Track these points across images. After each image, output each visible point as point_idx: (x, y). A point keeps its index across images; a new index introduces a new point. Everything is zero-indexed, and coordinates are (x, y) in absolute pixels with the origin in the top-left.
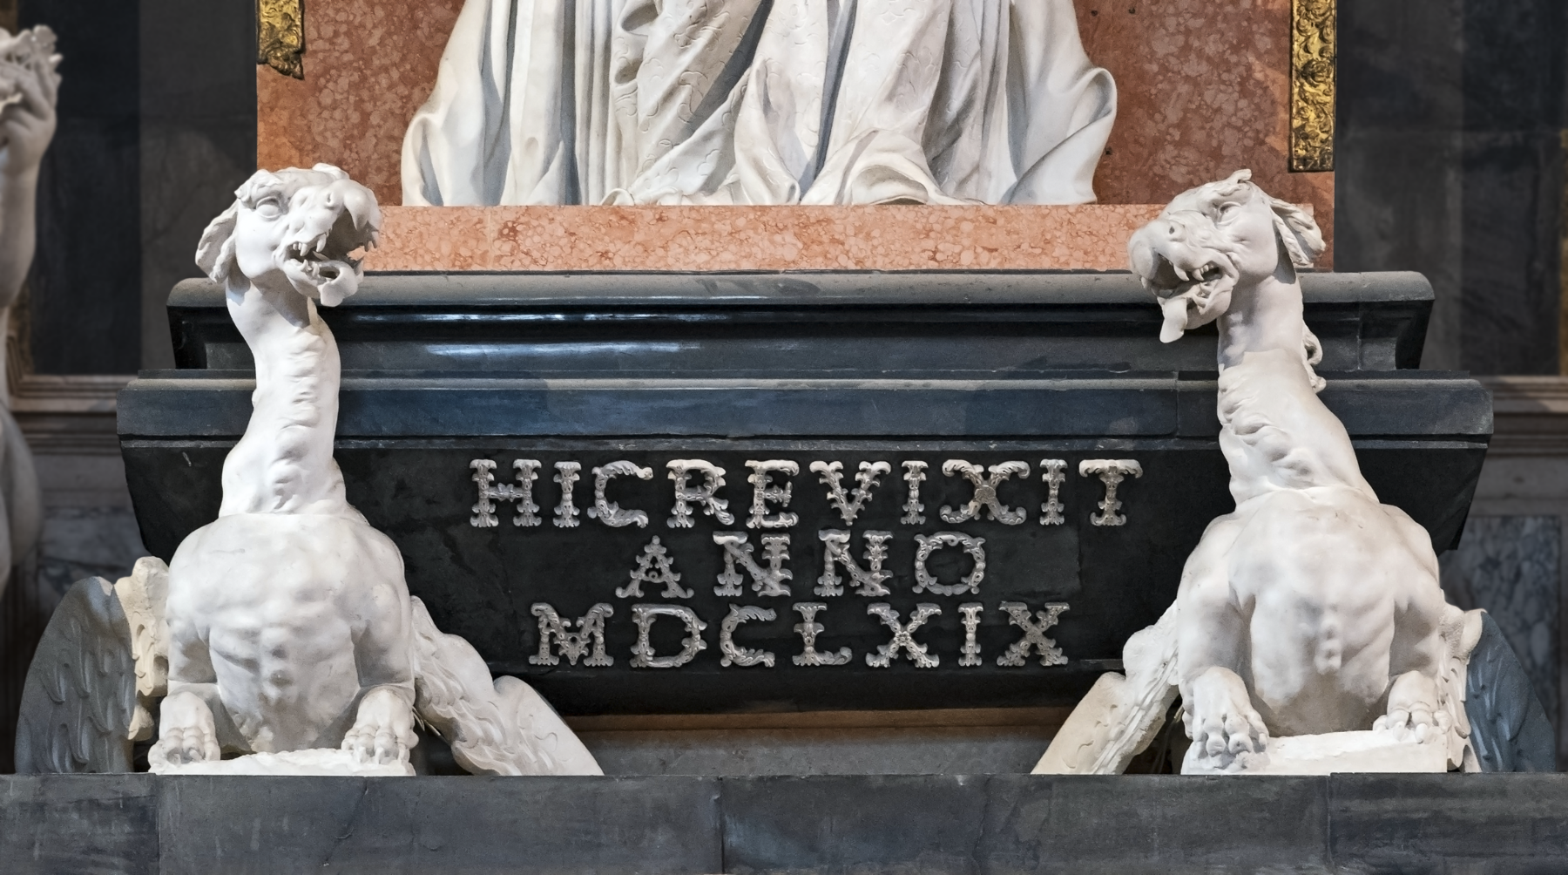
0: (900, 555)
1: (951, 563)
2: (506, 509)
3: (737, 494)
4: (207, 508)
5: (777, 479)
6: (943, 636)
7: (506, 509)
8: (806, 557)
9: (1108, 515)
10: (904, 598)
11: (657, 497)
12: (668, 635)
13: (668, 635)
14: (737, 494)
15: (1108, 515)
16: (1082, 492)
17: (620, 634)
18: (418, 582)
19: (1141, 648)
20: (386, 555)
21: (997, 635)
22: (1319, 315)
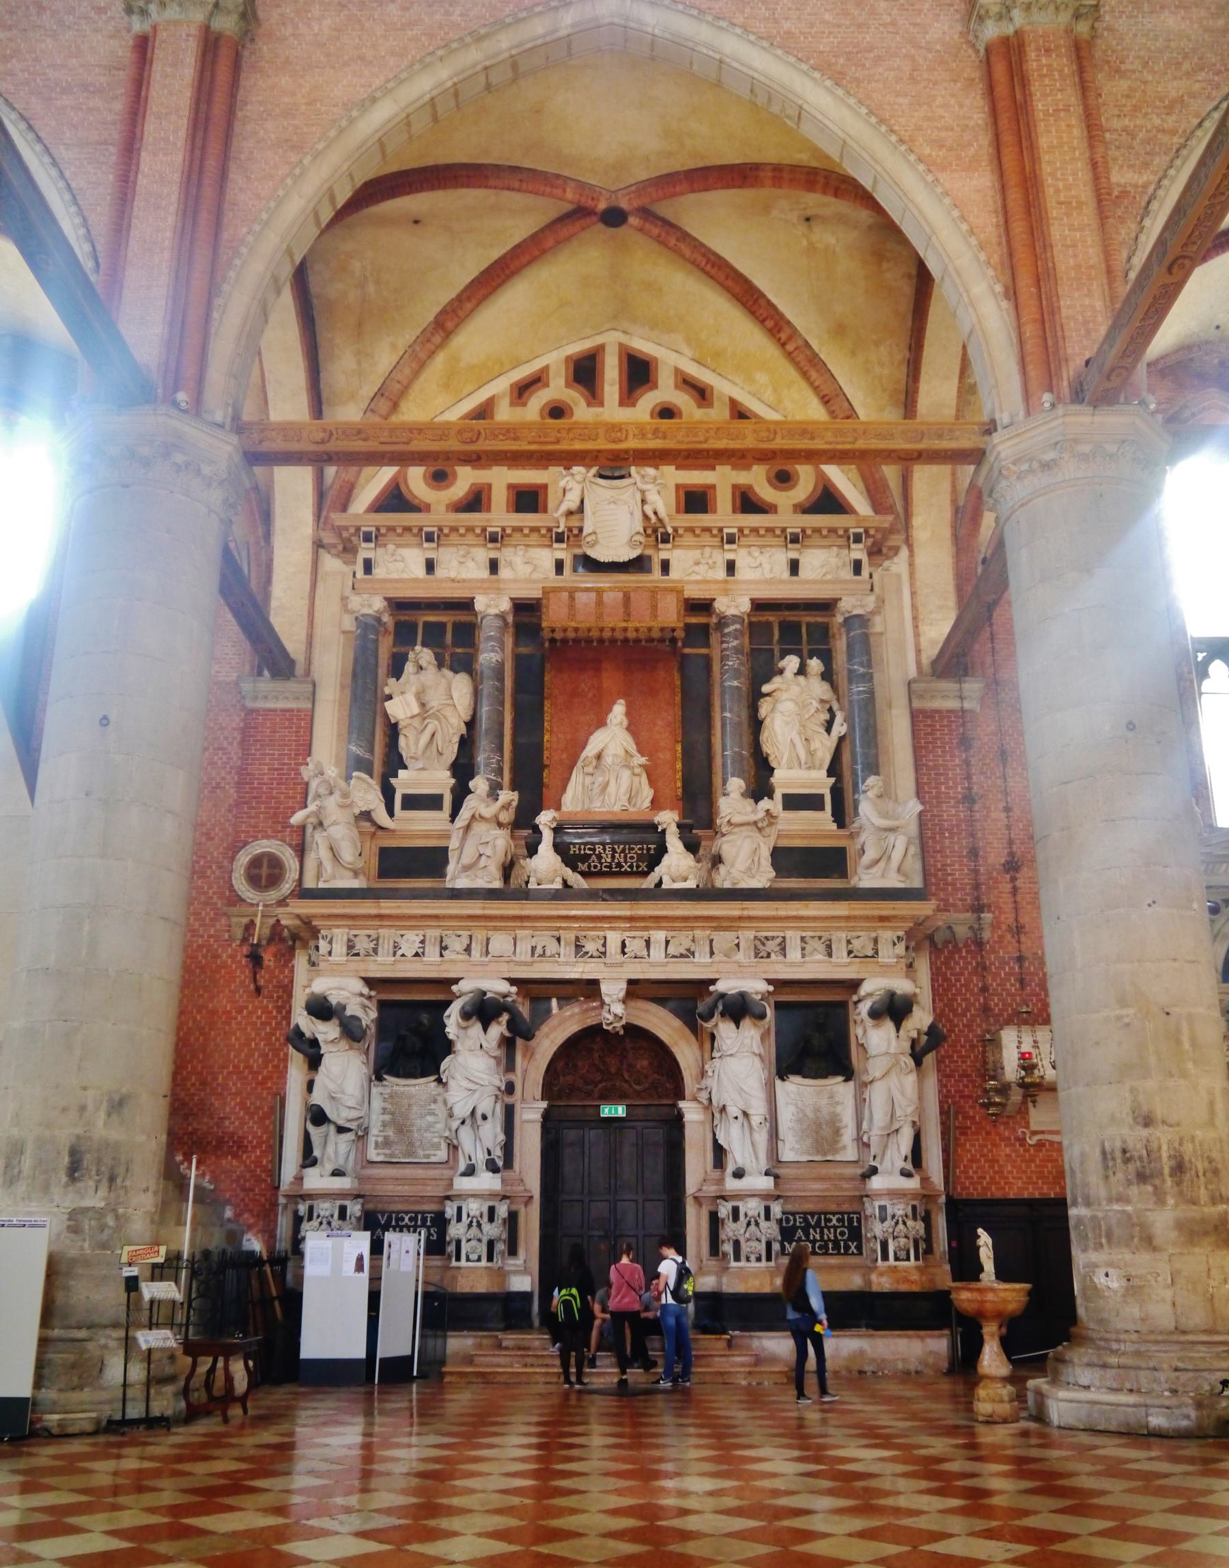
0: (625, 857)
1: (632, 858)
3: (604, 849)
4: (536, 852)
6: (631, 866)
8: (613, 857)
9: (652, 852)
10: (626, 862)
11: (594, 850)
12: (595, 867)
13: (595, 867)
14: (604, 849)
15: (652, 852)
16: (648, 849)
17: (589, 866)
18: (563, 861)
19: (657, 869)
20: (559, 859)
21: (638, 867)
22: (679, 826)
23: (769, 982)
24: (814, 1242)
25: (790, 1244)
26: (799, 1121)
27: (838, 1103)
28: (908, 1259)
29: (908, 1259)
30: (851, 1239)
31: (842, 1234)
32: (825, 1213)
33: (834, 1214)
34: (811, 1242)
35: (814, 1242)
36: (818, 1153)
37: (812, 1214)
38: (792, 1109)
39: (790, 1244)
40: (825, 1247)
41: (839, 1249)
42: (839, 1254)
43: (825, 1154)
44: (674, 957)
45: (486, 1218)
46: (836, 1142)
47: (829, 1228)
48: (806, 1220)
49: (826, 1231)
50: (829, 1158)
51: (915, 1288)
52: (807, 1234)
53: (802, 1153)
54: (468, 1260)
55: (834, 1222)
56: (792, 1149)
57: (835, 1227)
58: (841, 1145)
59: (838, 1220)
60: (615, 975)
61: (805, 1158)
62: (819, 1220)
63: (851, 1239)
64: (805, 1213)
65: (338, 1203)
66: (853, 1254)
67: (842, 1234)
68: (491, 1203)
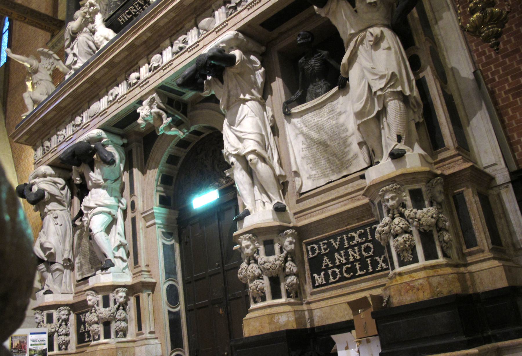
2: (122, 21)
5: (136, 4)
7: (122, 21)
23: (236, 31)
24: (340, 267)
25: (319, 274)
26: (309, 147)
27: (340, 114)
28: (416, 260)
29: (416, 260)
30: (375, 254)
31: (367, 249)
32: (347, 232)
33: (355, 230)
34: (338, 267)
35: (340, 267)
36: (333, 171)
37: (334, 237)
38: (301, 138)
39: (319, 274)
40: (352, 270)
41: (367, 268)
42: (367, 273)
43: (340, 172)
44: (177, 53)
45: (101, 304)
46: (347, 153)
47: (352, 247)
48: (329, 245)
49: (350, 250)
50: (345, 173)
51: (424, 296)
52: (333, 260)
53: (319, 178)
54: (94, 340)
55: (357, 239)
56: (309, 178)
57: (359, 244)
58: (351, 155)
59: (360, 236)
60: (147, 90)
61: (322, 182)
62: (342, 241)
63: (375, 254)
64: (328, 238)
65: (45, 313)
66: (383, 270)
67: (367, 249)
68: (105, 294)
